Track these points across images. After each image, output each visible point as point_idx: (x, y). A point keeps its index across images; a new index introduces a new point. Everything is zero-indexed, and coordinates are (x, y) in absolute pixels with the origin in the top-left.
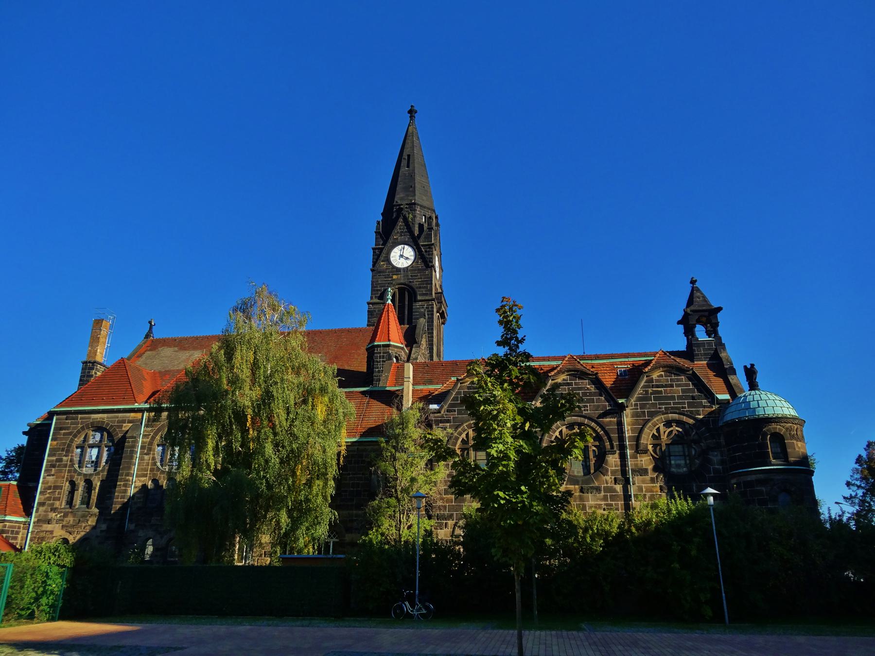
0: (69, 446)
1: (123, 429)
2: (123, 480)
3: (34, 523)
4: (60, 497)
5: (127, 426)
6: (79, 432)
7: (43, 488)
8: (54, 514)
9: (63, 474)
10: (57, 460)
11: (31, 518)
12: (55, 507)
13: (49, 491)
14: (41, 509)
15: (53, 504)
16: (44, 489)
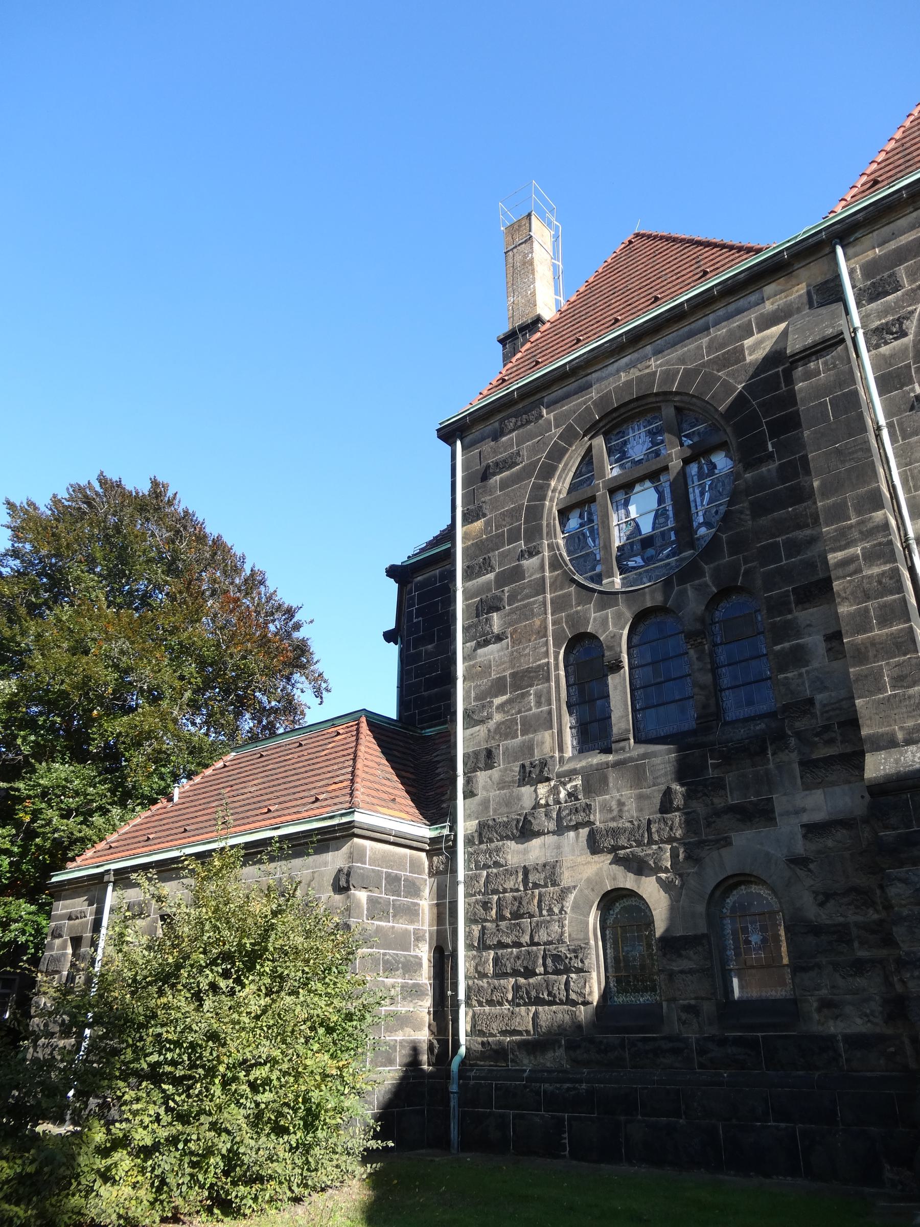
0: (535, 512)
1: (749, 359)
2: (856, 534)
3: (469, 841)
4: (550, 712)
5: (761, 342)
6: (557, 454)
7: (473, 695)
8: (543, 789)
9: (537, 622)
10: (502, 580)
11: (454, 822)
12: (537, 756)
13: (498, 701)
14: (482, 777)
15: (529, 748)
16: (477, 699)
